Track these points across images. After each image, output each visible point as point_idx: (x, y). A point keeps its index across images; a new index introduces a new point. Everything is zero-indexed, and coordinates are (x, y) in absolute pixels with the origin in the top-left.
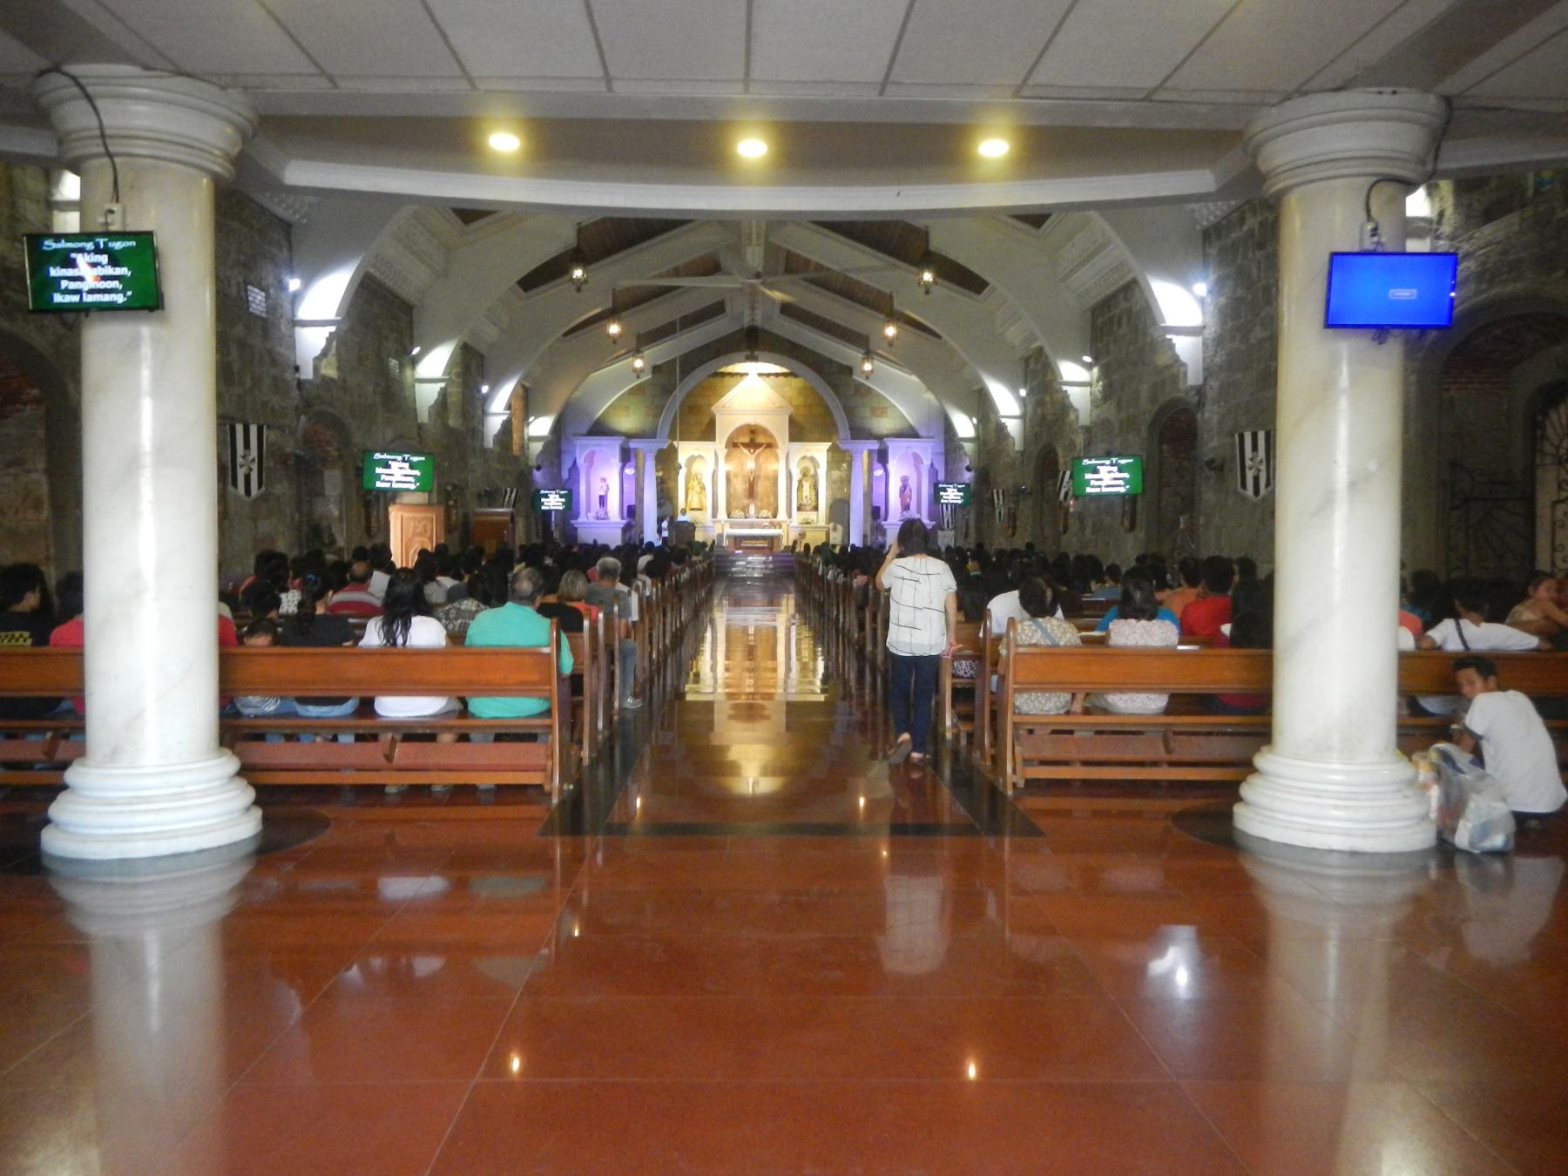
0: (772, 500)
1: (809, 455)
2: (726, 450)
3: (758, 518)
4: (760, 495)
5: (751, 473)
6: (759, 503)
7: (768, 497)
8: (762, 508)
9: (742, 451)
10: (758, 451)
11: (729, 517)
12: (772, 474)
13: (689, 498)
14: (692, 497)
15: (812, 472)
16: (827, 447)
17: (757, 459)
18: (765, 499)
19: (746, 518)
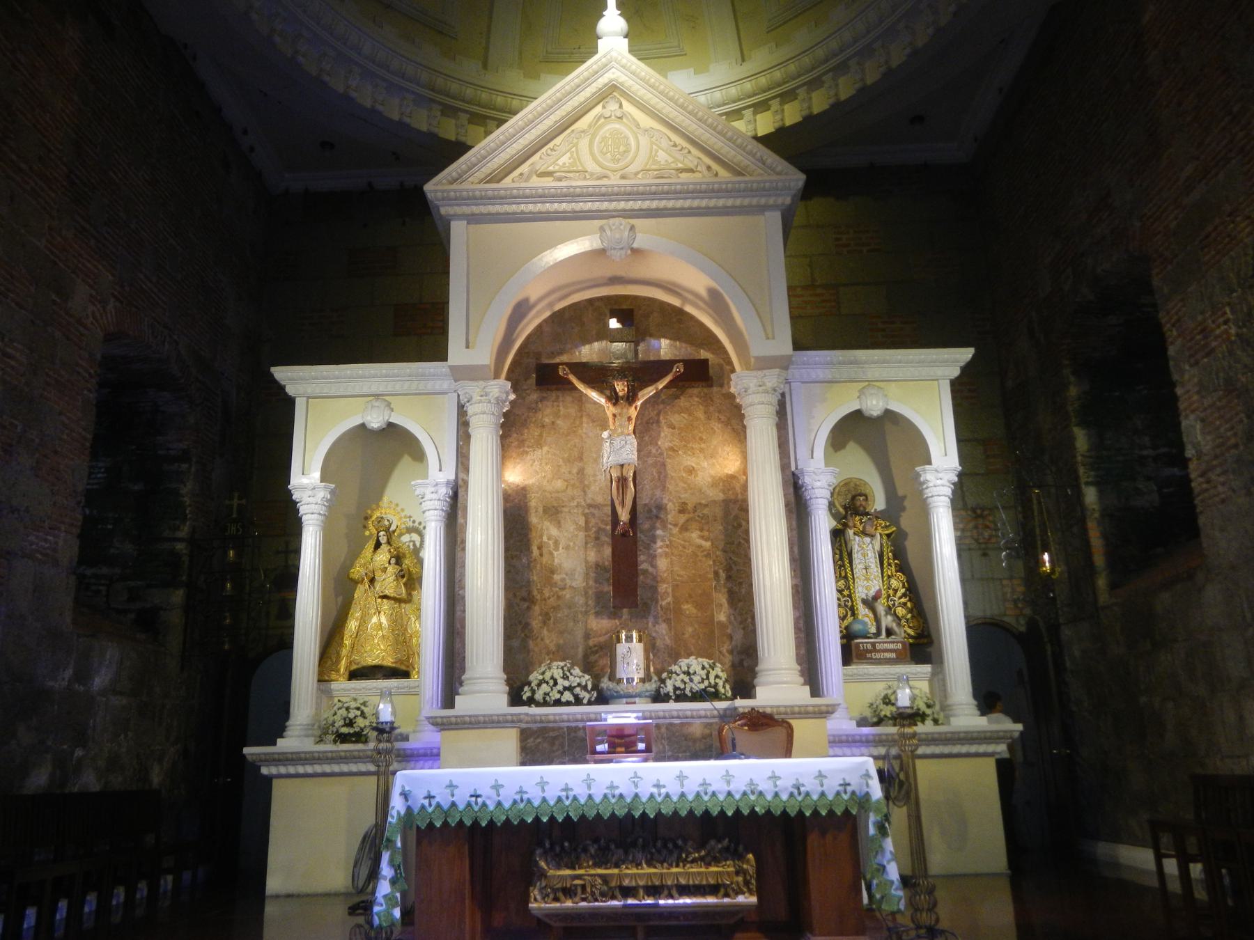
0: (722, 617)
1: (874, 406)
2: (500, 388)
3: (658, 697)
4: (663, 588)
5: (622, 481)
6: (662, 631)
7: (704, 603)
8: (675, 656)
9: (581, 399)
10: (648, 392)
11: (515, 699)
12: (717, 495)
13: (352, 625)
14: (363, 621)
15: (879, 503)
16: (956, 372)
17: (645, 430)
18: (688, 608)
19: (603, 699)
